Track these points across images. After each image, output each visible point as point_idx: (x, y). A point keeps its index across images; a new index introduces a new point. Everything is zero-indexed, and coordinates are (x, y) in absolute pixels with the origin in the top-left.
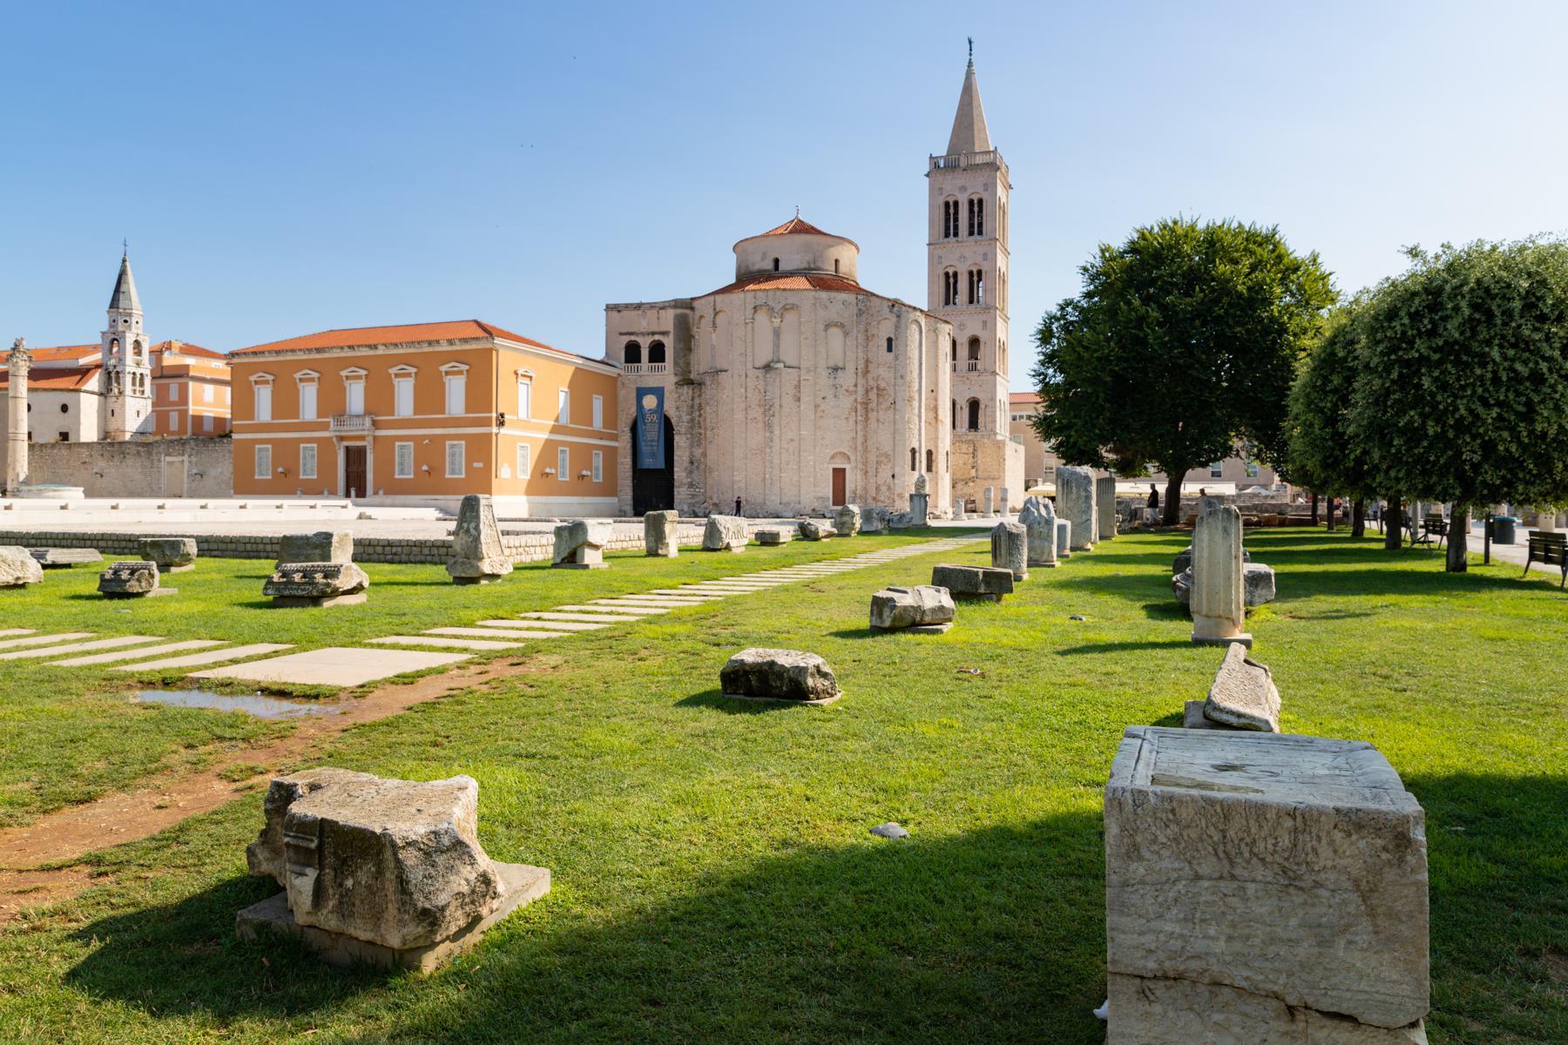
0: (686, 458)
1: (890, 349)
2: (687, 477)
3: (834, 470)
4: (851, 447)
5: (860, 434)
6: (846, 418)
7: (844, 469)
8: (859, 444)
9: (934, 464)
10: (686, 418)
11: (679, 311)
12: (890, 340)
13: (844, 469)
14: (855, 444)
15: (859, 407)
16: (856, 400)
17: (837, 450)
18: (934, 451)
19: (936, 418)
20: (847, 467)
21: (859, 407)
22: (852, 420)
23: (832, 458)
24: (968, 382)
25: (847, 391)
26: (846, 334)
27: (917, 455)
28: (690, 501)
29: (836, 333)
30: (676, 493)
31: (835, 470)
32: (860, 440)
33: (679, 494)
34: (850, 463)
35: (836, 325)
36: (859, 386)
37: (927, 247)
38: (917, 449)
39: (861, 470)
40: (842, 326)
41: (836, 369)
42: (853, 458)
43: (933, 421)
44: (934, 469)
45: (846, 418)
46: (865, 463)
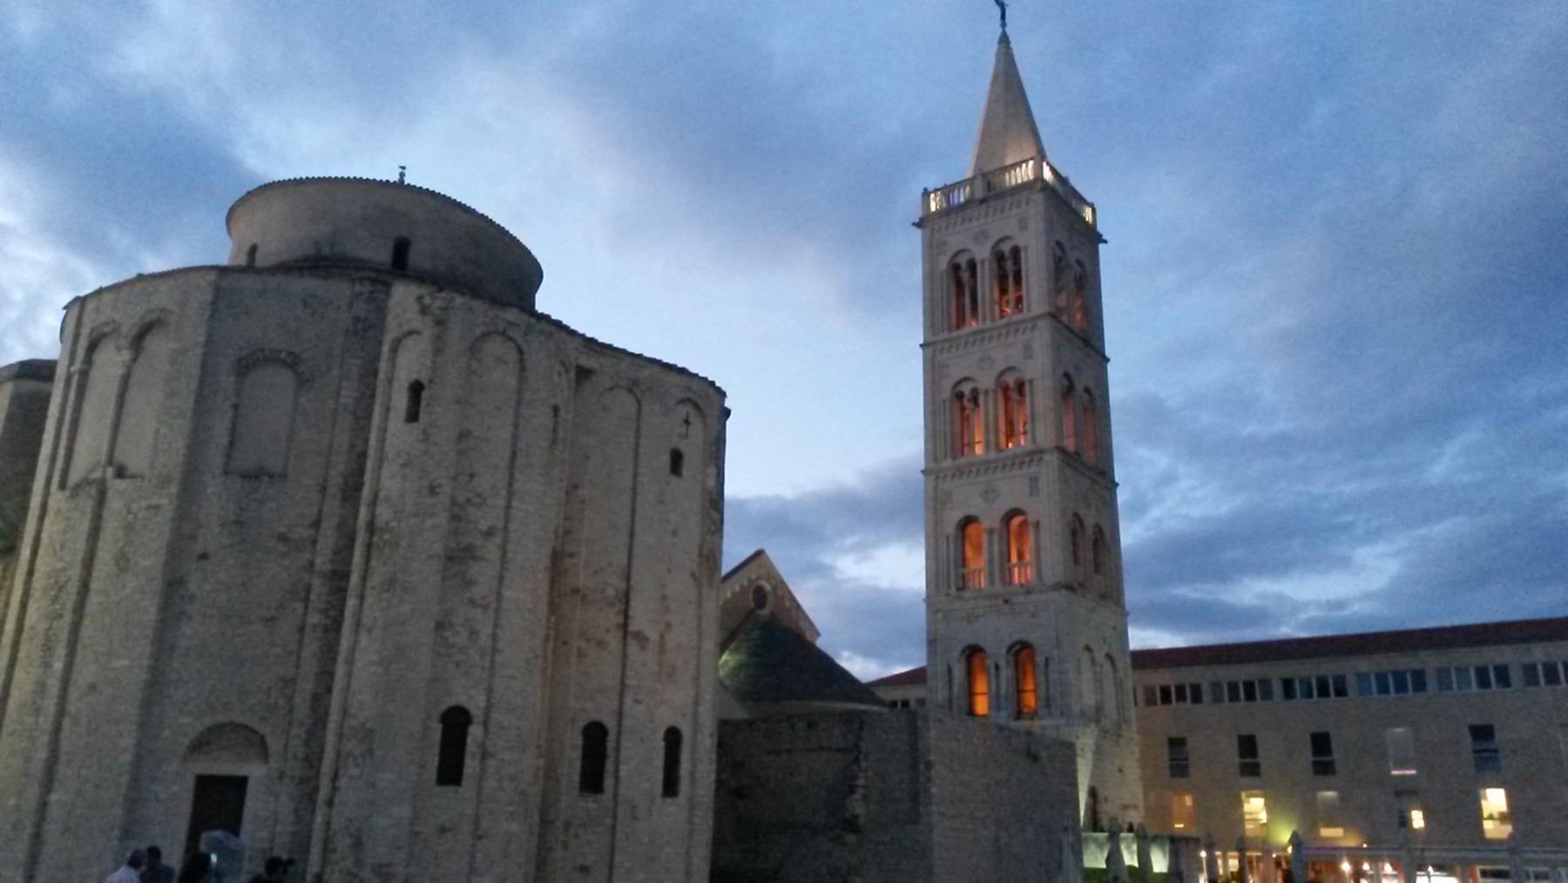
1: (413, 416)
5: (309, 667)
7: (242, 782)
9: (609, 766)
11: (29, 386)
12: (416, 389)
13: (242, 782)
14: (291, 699)
15: (316, 582)
16: (312, 564)
18: (610, 723)
19: (624, 626)
20: (255, 772)
21: (316, 582)
23: (199, 745)
24: (1006, 608)
25: (283, 538)
26: (303, 382)
27: (475, 731)
29: (275, 385)
32: (306, 686)
34: (265, 755)
35: (272, 359)
36: (325, 524)
37: (920, 351)
38: (476, 711)
40: (292, 362)
41: (256, 475)
42: (274, 744)
43: (614, 640)
44: (608, 782)
46: (312, 760)
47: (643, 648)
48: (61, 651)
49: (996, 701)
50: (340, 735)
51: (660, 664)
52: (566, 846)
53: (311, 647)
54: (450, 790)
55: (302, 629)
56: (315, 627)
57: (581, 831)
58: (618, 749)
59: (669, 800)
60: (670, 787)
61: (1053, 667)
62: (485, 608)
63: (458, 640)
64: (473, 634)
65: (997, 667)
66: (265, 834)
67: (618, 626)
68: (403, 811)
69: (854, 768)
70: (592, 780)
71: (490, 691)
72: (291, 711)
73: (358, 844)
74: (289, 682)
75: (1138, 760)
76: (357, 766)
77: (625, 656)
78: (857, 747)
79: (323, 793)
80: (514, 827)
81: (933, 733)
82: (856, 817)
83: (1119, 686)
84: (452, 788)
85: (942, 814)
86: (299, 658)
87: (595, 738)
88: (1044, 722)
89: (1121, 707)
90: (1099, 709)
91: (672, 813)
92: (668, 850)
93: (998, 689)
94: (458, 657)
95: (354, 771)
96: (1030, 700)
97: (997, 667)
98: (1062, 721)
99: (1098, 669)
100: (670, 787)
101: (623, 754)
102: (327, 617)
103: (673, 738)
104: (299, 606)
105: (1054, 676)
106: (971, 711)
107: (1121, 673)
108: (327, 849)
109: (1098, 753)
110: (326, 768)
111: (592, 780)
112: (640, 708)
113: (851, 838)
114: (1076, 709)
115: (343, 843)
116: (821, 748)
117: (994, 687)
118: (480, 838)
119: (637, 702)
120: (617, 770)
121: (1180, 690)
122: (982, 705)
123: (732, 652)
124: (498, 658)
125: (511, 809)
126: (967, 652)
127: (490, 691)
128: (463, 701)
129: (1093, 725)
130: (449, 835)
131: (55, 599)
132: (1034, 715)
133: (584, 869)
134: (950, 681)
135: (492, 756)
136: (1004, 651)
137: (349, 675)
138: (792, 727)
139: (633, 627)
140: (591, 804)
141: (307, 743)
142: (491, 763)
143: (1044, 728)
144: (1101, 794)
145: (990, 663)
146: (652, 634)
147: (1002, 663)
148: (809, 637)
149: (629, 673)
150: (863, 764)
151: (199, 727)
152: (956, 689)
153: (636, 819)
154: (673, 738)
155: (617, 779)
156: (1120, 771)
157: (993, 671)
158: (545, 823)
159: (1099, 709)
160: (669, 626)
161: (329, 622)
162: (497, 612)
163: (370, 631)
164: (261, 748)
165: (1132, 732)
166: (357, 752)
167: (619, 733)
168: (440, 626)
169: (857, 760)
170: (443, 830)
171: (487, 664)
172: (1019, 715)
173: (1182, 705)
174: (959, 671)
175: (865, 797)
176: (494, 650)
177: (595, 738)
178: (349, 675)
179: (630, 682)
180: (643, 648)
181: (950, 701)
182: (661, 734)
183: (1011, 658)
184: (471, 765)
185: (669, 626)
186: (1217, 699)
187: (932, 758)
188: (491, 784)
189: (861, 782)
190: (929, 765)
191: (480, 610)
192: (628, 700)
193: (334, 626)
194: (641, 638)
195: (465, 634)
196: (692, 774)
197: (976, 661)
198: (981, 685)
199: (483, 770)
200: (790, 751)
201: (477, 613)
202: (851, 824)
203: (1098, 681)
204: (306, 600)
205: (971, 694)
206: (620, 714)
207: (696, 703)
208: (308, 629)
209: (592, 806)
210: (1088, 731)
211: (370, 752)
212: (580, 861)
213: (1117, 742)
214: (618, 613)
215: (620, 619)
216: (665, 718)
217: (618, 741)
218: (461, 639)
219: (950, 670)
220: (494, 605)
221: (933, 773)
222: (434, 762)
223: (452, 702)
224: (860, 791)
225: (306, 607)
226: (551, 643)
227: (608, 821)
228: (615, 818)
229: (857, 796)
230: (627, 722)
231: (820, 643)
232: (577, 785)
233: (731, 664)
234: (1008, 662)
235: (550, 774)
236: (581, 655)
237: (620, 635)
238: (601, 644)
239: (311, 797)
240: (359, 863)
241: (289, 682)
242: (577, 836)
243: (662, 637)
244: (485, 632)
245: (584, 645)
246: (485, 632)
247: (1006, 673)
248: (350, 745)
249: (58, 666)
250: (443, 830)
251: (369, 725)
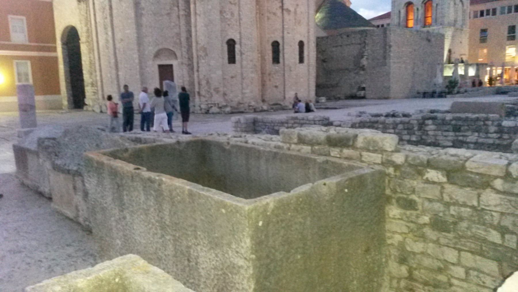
0: (88, 63)
2: (91, 78)
3: (160, 67)
4: (175, 43)
5: (183, 28)
6: (168, 14)
7: (171, 66)
8: (182, 39)
9: (281, 55)
10: (85, 29)
13: (171, 66)
14: (180, 40)
17: (161, 47)
18: (280, 41)
19: (282, 7)
20: (175, 63)
22: (174, 15)
23: (157, 55)
27: (237, 47)
28: (94, 97)
30: (86, 91)
31: (160, 67)
32: (184, 35)
33: (88, 92)
34: (176, 58)
38: (237, 40)
39: (189, 65)
42: (178, 54)
43: (279, 12)
44: (281, 60)
45: (168, 14)
46: (190, 58)
47: (289, 14)
48: (109, 29)
49: (416, 21)
50: (197, 50)
51: (295, 19)
52: (270, 80)
53: (183, 22)
54: (232, 65)
55: (179, 17)
56: (182, 15)
57: (274, 75)
58: (283, 49)
59: (301, 64)
60: (301, 60)
61: (439, 7)
62: (235, 4)
63: (228, 16)
64: (232, 14)
65: (418, 9)
66: (181, 81)
67: (280, 7)
68: (220, 72)
69: (364, 50)
70: (276, 60)
71: (240, 33)
72: (181, 43)
73: (208, 82)
74: (178, 35)
75: (468, 38)
76: (203, 59)
77: (283, 17)
78: (365, 42)
79: (195, 69)
80: (253, 75)
81: (392, 35)
82: (364, 66)
83: (464, 11)
84: (233, 65)
85: (394, 62)
86: (180, 26)
87: (276, 46)
88: (435, 28)
89: (464, 20)
90: (455, 21)
91: (302, 68)
92: (302, 80)
93: (418, 17)
94: (229, 22)
95: (203, 61)
96: (429, 20)
97: (418, 9)
98: (441, 27)
99: (456, 6)
100: (301, 60)
101: (285, 51)
102: (186, 11)
103: (301, 44)
104: (176, 8)
105: (439, 11)
106: (407, 27)
107: (465, 8)
108: (199, 84)
109: (453, 37)
110: (195, 61)
111: (276, 60)
112: (289, 35)
113: (362, 72)
114: (446, 22)
115: (204, 83)
116: (352, 44)
117: (416, 16)
118: (243, 79)
119: (288, 33)
120: (284, 56)
121: (488, 11)
122: (411, 24)
123: (320, 13)
124: (241, 22)
125: (251, 70)
126: (407, 5)
127: (240, 33)
128: (233, 37)
129: (452, 27)
130: (234, 79)
131: (103, 12)
132: (430, 25)
133: (276, 87)
134: (399, 17)
135: (244, 54)
136: (421, 2)
137: (196, 31)
138: (342, 38)
139: (285, 7)
140: (277, 67)
141: (188, 53)
142: (244, 56)
143: (434, 30)
144: (453, 51)
145: (415, 8)
146: (292, 9)
147: (420, 8)
148: (347, 4)
149: (285, 23)
150: (367, 48)
151: (156, 49)
152: (402, 19)
153: (291, 71)
154: (301, 44)
155: (284, 59)
156: (461, 42)
157: (416, 11)
158: (263, 73)
159: (455, 21)
160: (297, 5)
161: (186, 13)
162: (239, 7)
163: (200, 15)
164: (174, 55)
165: (467, 29)
166: (203, 55)
167: (283, 44)
168: (221, 12)
169: (364, 47)
170: (232, 77)
171: (238, 24)
172: (425, 26)
173: (488, 17)
174: (403, 12)
175: (367, 59)
176: (240, 19)
177: (276, 46)
178: (196, 31)
179: (286, 27)
180: (289, 14)
181: (399, 24)
182: (297, 43)
183: (423, 5)
184: (238, 57)
185: (297, 5)
186: (502, 13)
187: (391, 44)
188: (244, 63)
189: (366, 54)
190: (390, 46)
191: (233, 5)
192: (285, 32)
193: (188, 15)
194: (288, 11)
195: (229, 14)
196: (308, 56)
197: (410, 7)
198: (411, 17)
199: (242, 59)
200: (341, 46)
201: (233, 7)
202: (363, 68)
203: (456, 12)
204: (178, 7)
205: (407, 20)
206: (283, 38)
207: (309, 32)
208: (181, 17)
209: (277, 68)
210: (450, 29)
211: (207, 55)
212: (275, 84)
213: (461, 32)
214: (279, 2)
215: (281, 4)
216: (298, 38)
217: (283, 46)
218: (229, 16)
219: (400, 12)
220: (238, 3)
221: (392, 49)
222: (226, 56)
223: (228, 38)
224: (366, 57)
225: (178, 8)
226: (258, 15)
227: (282, 72)
228: (284, 71)
229: (364, 59)
230: (286, 40)
231: (352, 7)
232: (271, 62)
233: (320, 17)
234: (422, 6)
235: (263, 58)
236: (268, 19)
237: (280, 11)
238: (275, 14)
239: (192, 69)
240: (209, 88)
241: (178, 35)
242: (273, 77)
243: (295, 10)
244: (236, 13)
245: (269, 15)
246: (236, 13)
247: (421, 11)
248: (201, 53)
249: (110, 33)
250: (232, 77)
251: (205, 46)
